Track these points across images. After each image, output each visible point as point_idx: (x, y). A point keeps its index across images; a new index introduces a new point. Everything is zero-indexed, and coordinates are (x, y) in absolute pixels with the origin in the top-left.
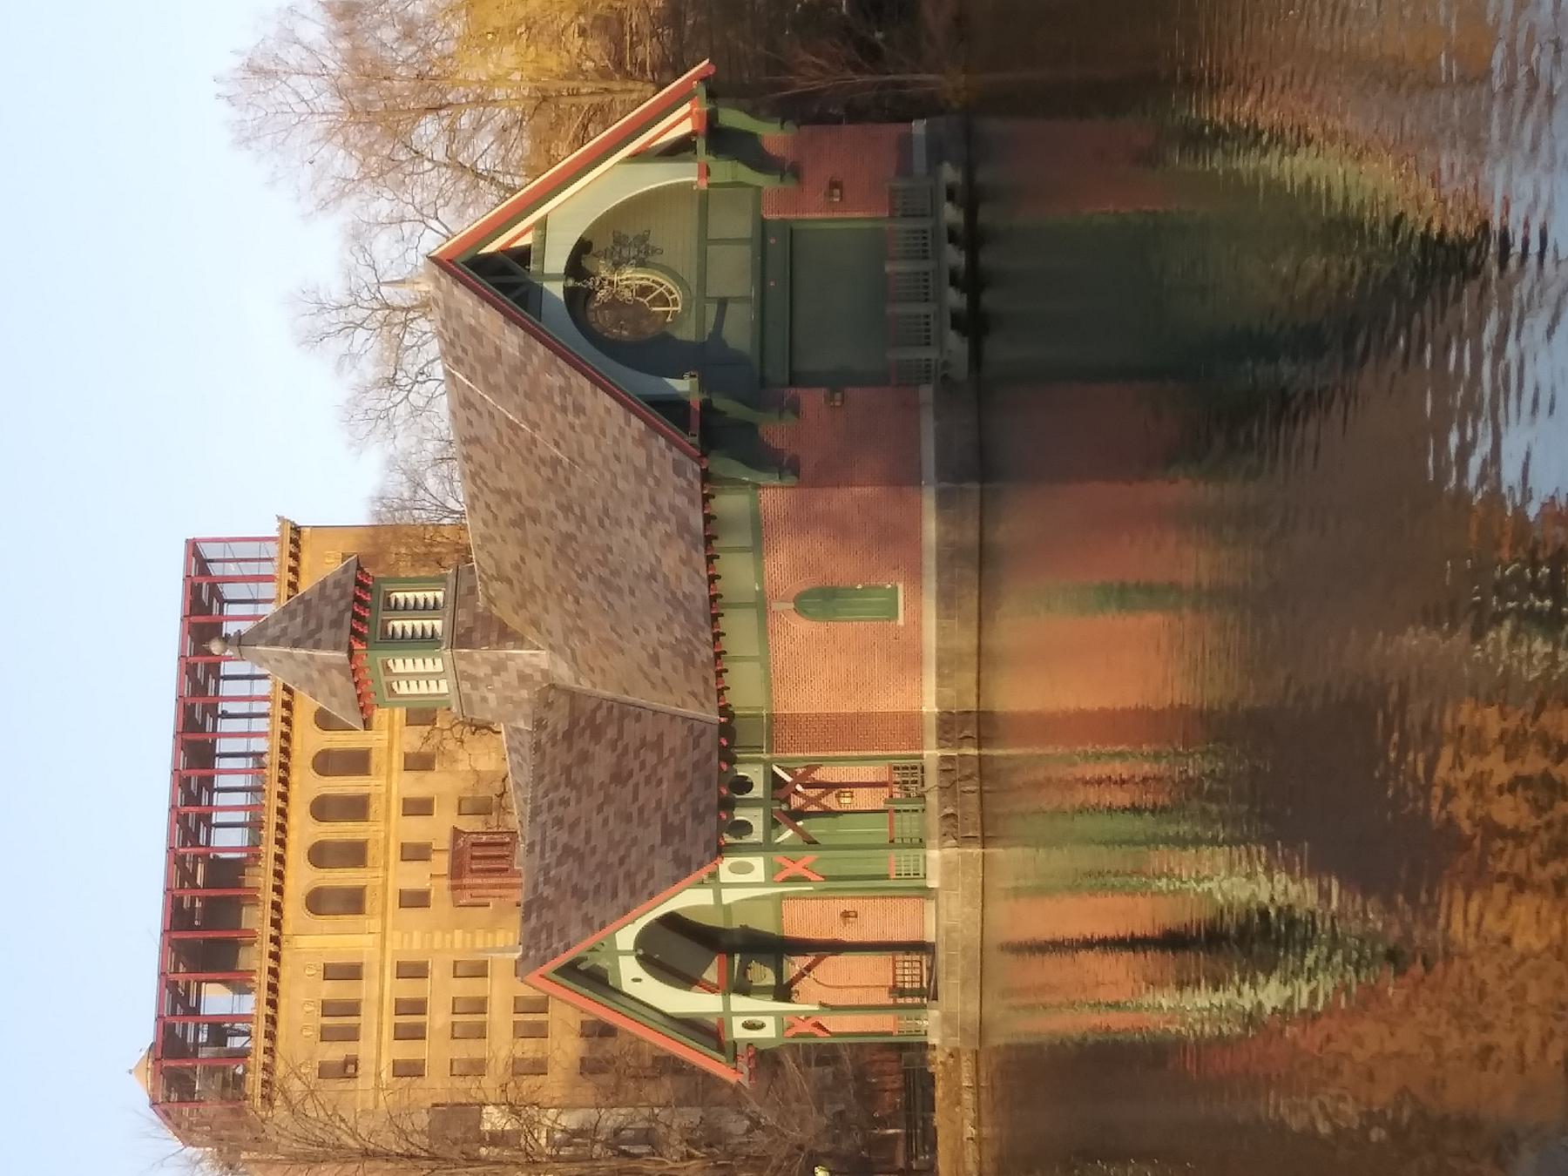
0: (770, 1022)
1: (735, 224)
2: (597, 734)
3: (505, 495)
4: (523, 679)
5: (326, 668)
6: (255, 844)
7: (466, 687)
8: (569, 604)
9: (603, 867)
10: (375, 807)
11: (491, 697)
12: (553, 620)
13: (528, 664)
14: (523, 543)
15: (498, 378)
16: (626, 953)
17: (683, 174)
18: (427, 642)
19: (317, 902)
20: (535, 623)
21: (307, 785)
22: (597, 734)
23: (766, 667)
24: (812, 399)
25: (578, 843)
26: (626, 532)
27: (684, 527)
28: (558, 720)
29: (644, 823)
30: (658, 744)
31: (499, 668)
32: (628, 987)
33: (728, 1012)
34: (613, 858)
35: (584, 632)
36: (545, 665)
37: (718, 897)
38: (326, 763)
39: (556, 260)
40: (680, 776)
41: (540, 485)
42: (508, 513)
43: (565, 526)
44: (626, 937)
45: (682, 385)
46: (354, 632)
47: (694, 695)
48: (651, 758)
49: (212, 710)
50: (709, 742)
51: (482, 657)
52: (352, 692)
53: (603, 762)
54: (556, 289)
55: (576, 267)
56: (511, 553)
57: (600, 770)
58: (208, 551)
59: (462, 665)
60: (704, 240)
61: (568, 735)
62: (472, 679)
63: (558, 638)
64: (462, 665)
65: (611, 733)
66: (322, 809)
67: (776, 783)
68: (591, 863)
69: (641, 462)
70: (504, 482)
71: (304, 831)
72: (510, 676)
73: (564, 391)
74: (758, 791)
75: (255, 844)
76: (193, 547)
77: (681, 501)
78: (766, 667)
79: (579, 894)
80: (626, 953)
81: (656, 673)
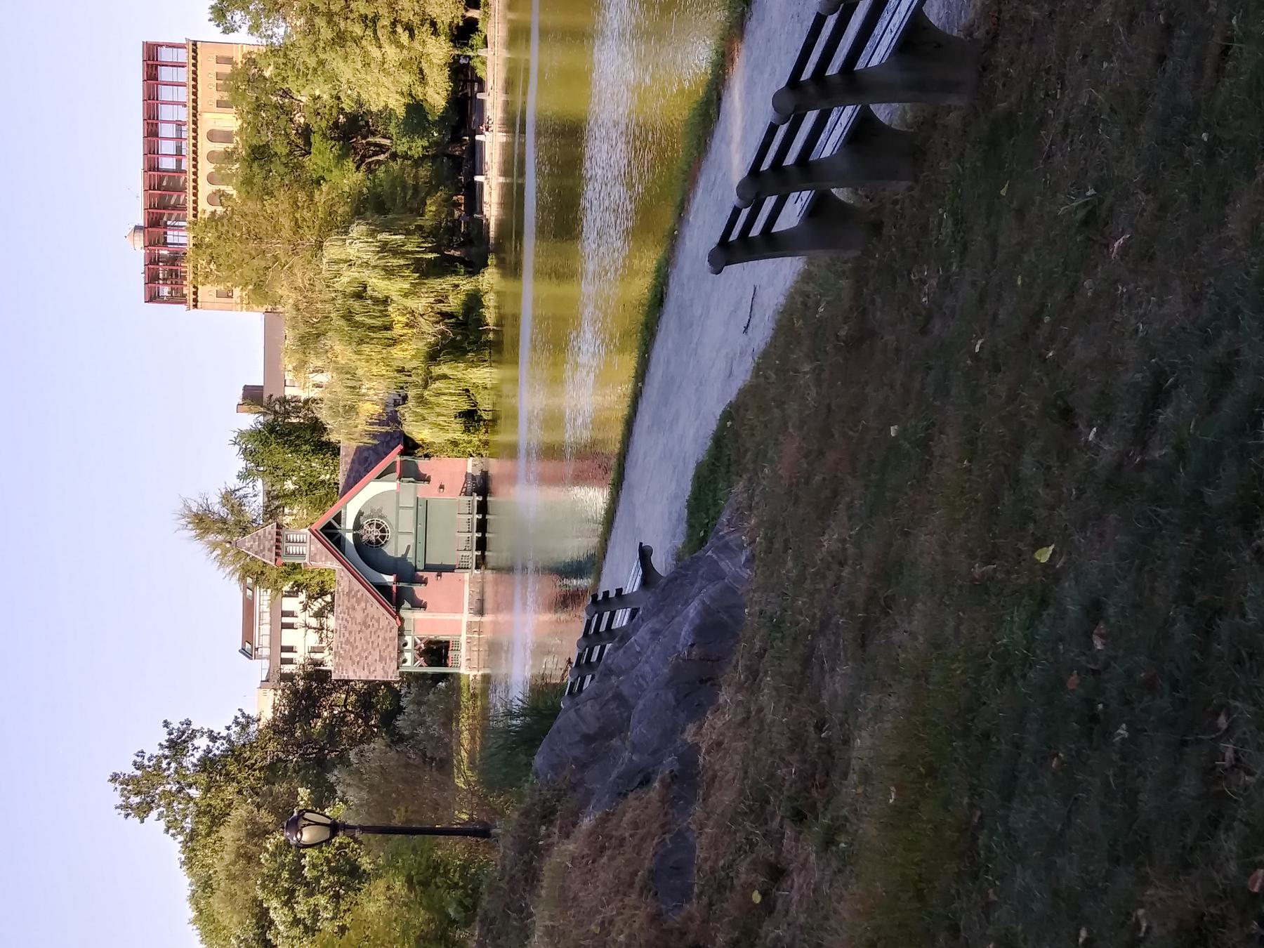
2: (358, 601)
6: (179, 162)
17: (390, 485)
24: (431, 576)
30: (378, 621)
34: (364, 655)
39: (349, 523)
40: (385, 639)
45: (389, 579)
46: (277, 554)
50: (395, 631)
54: (349, 537)
55: (358, 525)
60: (399, 508)
61: (348, 594)
65: (363, 604)
75: (179, 162)
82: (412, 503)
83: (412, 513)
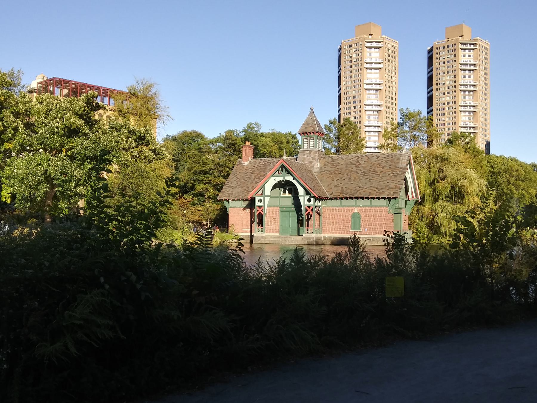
3: (358, 162)
5: (314, 128)
7: (308, 152)
11: (305, 156)
12: (329, 168)
13: (315, 164)
16: (284, 178)
18: (315, 145)
31: (313, 158)
32: (273, 178)
35: (331, 174)
36: (315, 166)
41: (368, 168)
47: (332, 193)
59: (313, 152)
62: (310, 153)
64: (313, 152)
72: (311, 160)
80: (284, 178)
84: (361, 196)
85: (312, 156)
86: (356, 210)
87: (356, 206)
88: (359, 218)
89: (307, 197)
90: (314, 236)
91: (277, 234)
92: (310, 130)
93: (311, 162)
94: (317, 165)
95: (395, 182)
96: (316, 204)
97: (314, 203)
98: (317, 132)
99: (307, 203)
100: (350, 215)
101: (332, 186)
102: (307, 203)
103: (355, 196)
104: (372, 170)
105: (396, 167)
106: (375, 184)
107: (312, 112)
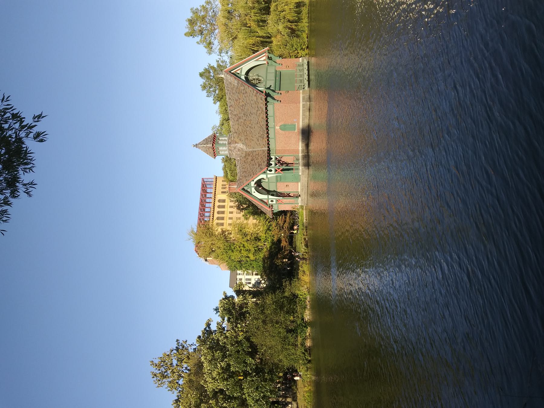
0: (275, 200)
1: (272, 70)
4: (239, 150)
8: (245, 134)
9: (249, 172)
10: (226, 212)
12: (243, 138)
14: (238, 124)
15: (234, 91)
18: (224, 145)
19: (217, 224)
20: (240, 140)
21: (217, 209)
22: (249, 155)
23: (275, 140)
25: (246, 170)
26: (253, 116)
27: (262, 111)
28: (244, 155)
29: (256, 165)
32: (253, 194)
33: (268, 199)
37: (267, 176)
38: (219, 207)
39: (244, 73)
41: (240, 110)
42: (236, 119)
43: (244, 118)
44: (253, 184)
48: (257, 156)
49: (205, 201)
50: (266, 152)
51: (232, 145)
52: (213, 152)
53: (250, 158)
56: (236, 127)
57: (249, 160)
58: (205, 180)
62: (231, 150)
63: (244, 142)
65: (251, 155)
66: (218, 213)
67: (276, 158)
68: (247, 172)
69: (256, 100)
70: (235, 113)
71: (216, 215)
72: (237, 150)
73: (244, 90)
74: (273, 159)
76: (203, 179)
77: (262, 105)
78: (275, 140)
79: (245, 177)
81: (258, 143)
82: (274, 71)
83: (274, 75)
84: (265, 126)
85: (233, 149)
86: (277, 128)
87: (274, 127)
88: (285, 125)
89: (268, 172)
90: (300, 160)
91: (299, 184)
92: (211, 150)
93: (239, 150)
94: (240, 145)
95: (251, 95)
96: (273, 165)
97: (272, 167)
98: (213, 145)
99: (273, 172)
100: (283, 132)
101: (258, 143)
102: (273, 172)
103: (265, 129)
104: (241, 108)
105: (237, 88)
106: (255, 111)
107: (196, 146)
